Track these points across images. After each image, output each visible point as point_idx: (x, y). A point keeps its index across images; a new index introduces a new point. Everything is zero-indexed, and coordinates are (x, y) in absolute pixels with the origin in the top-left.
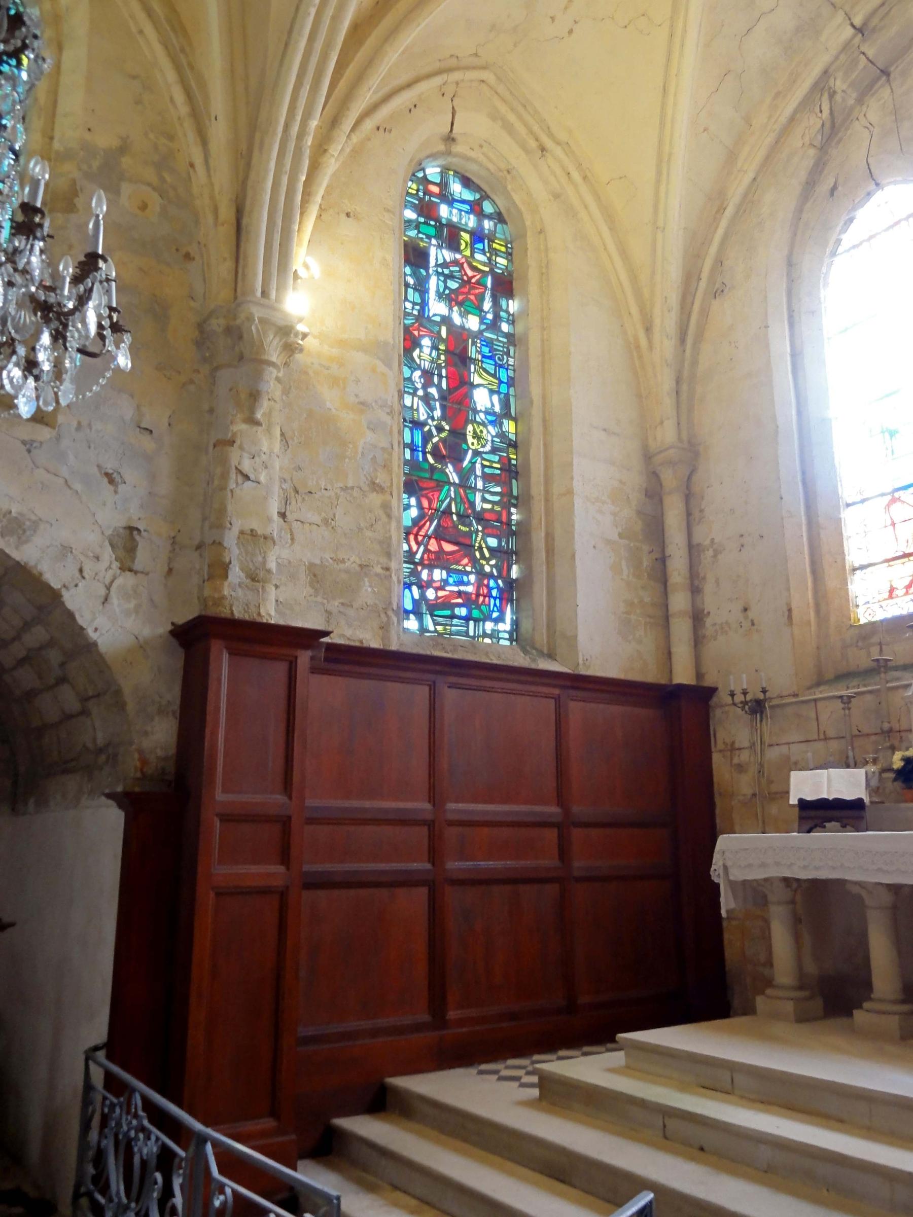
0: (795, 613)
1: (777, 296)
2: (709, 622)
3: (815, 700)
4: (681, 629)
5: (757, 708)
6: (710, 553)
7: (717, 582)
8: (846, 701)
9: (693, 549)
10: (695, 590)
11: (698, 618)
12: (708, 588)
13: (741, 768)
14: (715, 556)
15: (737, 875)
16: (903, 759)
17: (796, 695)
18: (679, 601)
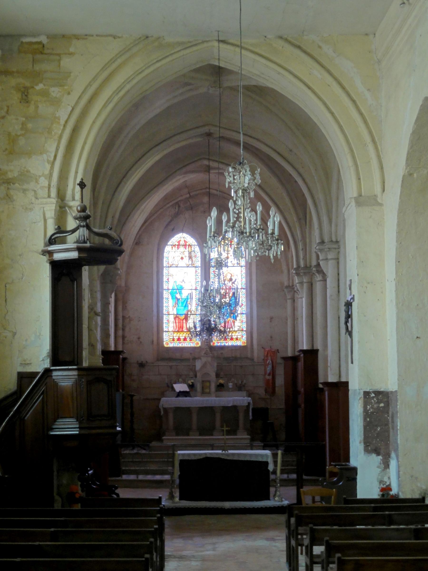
0: (154, 342)
1: (155, 252)
2: (126, 339)
3: (158, 365)
4: (120, 341)
5: (142, 365)
6: (128, 320)
7: (130, 328)
8: (171, 367)
9: (123, 317)
10: (123, 330)
11: (124, 337)
12: (127, 329)
13: (133, 380)
14: (130, 320)
15: (166, 406)
16: (192, 382)
17: (153, 363)
18: (120, 333)
